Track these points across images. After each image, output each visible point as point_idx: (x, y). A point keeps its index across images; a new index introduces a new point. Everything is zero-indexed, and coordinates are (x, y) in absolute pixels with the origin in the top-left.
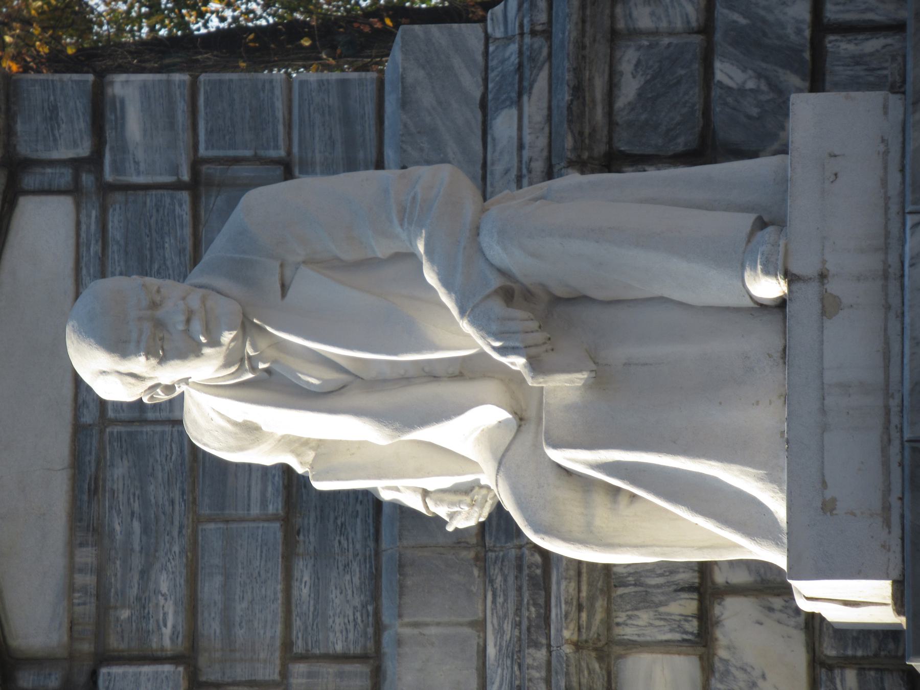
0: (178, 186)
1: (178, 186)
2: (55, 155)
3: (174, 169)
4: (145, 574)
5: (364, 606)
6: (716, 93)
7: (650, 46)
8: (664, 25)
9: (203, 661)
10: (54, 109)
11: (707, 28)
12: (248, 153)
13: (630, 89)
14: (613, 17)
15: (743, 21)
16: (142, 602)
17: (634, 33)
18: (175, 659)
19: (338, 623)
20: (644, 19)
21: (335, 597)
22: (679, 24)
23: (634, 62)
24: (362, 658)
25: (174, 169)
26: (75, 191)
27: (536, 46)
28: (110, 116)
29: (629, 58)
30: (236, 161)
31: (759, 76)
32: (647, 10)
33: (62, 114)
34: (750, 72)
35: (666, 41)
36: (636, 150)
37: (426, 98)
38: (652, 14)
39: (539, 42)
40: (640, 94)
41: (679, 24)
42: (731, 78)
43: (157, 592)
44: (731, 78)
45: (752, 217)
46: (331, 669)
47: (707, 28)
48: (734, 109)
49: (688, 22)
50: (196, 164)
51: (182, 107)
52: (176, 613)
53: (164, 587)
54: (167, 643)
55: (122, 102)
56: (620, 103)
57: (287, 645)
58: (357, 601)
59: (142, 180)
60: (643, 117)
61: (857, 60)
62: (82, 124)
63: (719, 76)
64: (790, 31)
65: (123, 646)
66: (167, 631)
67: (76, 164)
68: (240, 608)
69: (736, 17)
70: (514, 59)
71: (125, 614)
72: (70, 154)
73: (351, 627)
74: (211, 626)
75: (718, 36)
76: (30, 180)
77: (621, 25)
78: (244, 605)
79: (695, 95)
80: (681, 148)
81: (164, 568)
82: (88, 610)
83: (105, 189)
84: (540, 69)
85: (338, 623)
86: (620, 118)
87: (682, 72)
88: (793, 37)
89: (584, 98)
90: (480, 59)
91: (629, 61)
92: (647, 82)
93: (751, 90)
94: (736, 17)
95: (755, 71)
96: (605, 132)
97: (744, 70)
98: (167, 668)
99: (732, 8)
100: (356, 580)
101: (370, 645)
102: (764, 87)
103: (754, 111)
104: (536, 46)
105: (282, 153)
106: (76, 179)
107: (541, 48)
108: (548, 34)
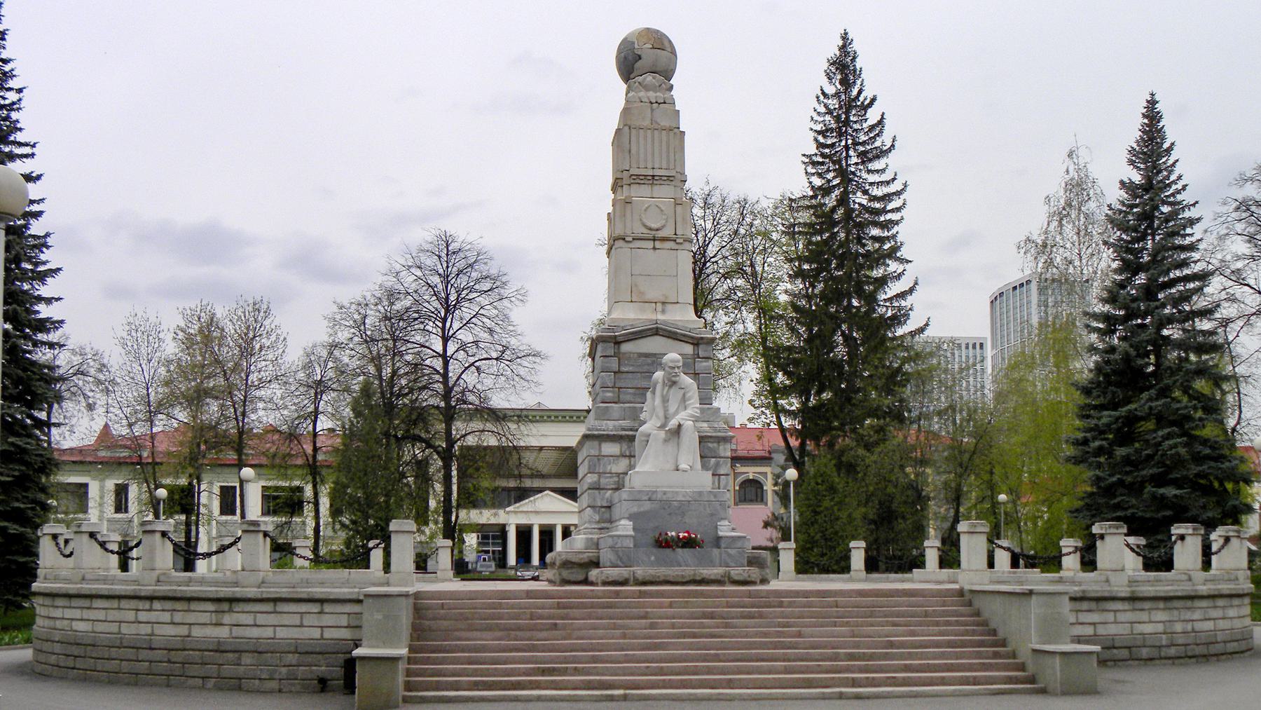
74: (624, 375)
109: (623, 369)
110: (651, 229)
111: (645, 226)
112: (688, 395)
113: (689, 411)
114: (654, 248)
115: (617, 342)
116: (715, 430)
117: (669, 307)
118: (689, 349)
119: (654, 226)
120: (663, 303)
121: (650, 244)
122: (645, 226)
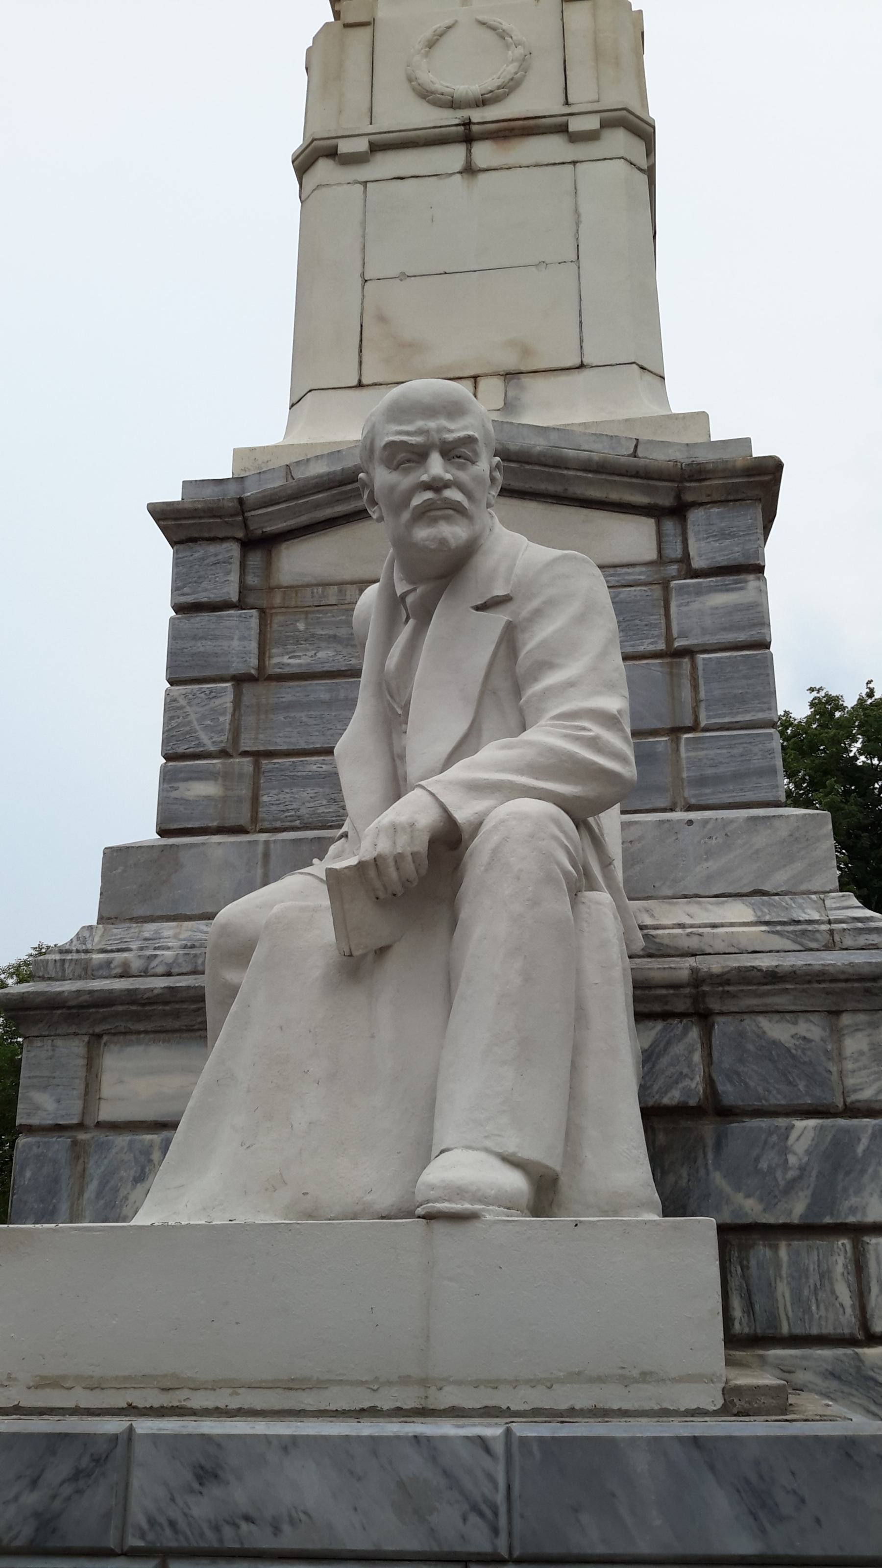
0: (669, 639)
1: (669, 639)
2: (691, 542)
3: (683, 635)
4: (334, 638)
5: (299, 817)
6: (782, 1122)
7: (826, 1052)
8: (849, 1065)
9: (260, 689)
10: (732, 536)
11: (853, 1111)
12: (702, 695)
13: (779, 1031)
14: (855, 1011)
15: (860, 1149)
16: (311, 639)
17: (837, 1034)
18: (261, 667)
19: (285, 797)
20: (855, 1044)
21: (306, 793)
22: (850, 1082)
23: (808, 1035)
24: (254, 819)
25: (683, 635)
26: (661, 560)
27: (818, 935)
28: (729, 579)
29: (812, 1029)
30: (695, 687)
31: (802, 1169)
32: (865, 1048)
33: (727, 542)
34: (805, 1159)
35: (834, 1069)
36: (716, 1041)
37: (761, 839)
38: (861, 1053)
39: (824, 938)
40: (776, 1043)
41: (850, 1082)
42: (798, 1139)
43: (319, 649)
44: (798, 1139)
45: (554, 1162)
46: (245, 791)
47: (853, 1111)
48: (766, 1142)
49: (855, 1091)
50: (688, 652)
51: (742, 636)
52: (300, 665)
53: (320, 655)
54: (275, 660)
55: (742, 589)
56: (764, 1022)
57: (270, 754)
58: (303, 811)
59: (673, 609)
60: (751, 1047)
61: (825, 1275)
62: (721, 559)
63: (800, 1124)
64: (854, 1201)
65: (275, 626)
66: (286, 660)
67: (686, 558)
68: (303, 716)
69: (864, 1142)
70: (803, 917)
71: (301, 626)
72: (692, 552)
73: (282, 807)
74: (289, 692)
75: (842, 1122)
76: (669, 526)
77: (846, 1019)
78: (304, 719)
79: (777, 1099)
80: (720, 1088)
81: (338, 653)
82: (307, 598)
83: (665, 585)
84: (795, 942)
85: (285, 797)
86: (749, 1024)
87: (801, 1086)
88: (847, 1204)
89: (766, 984)
90: (804, 887)
91: (808, 1030)
92: (788, 1050)
93: (786, 1161)
94: (864, 1142)
95: (807, 1164)
96: (733, 1009)
97: (808, 1152)
98: (254, 661)
99: (874, 1136)
100: (321, 810)
101: (266, 825)
102: (790, 1174)
103: (764, 1165)
104: (818, 935)
105: (703, 723)
106: (672, 562)
107: (816, 940)
108: (830, 947)
109: (283, 660)
110: (453, 104)
111: (426, 95)
112: (532, 641)
113: (544, 735)
114: (469, 170)
115: (261, 544)
116: (802, 933)
117: (538, 387)
118: (633, 539)
119: (467, 86)
120: (510, 376)
121: (453, 157)
122: (426, 95)
